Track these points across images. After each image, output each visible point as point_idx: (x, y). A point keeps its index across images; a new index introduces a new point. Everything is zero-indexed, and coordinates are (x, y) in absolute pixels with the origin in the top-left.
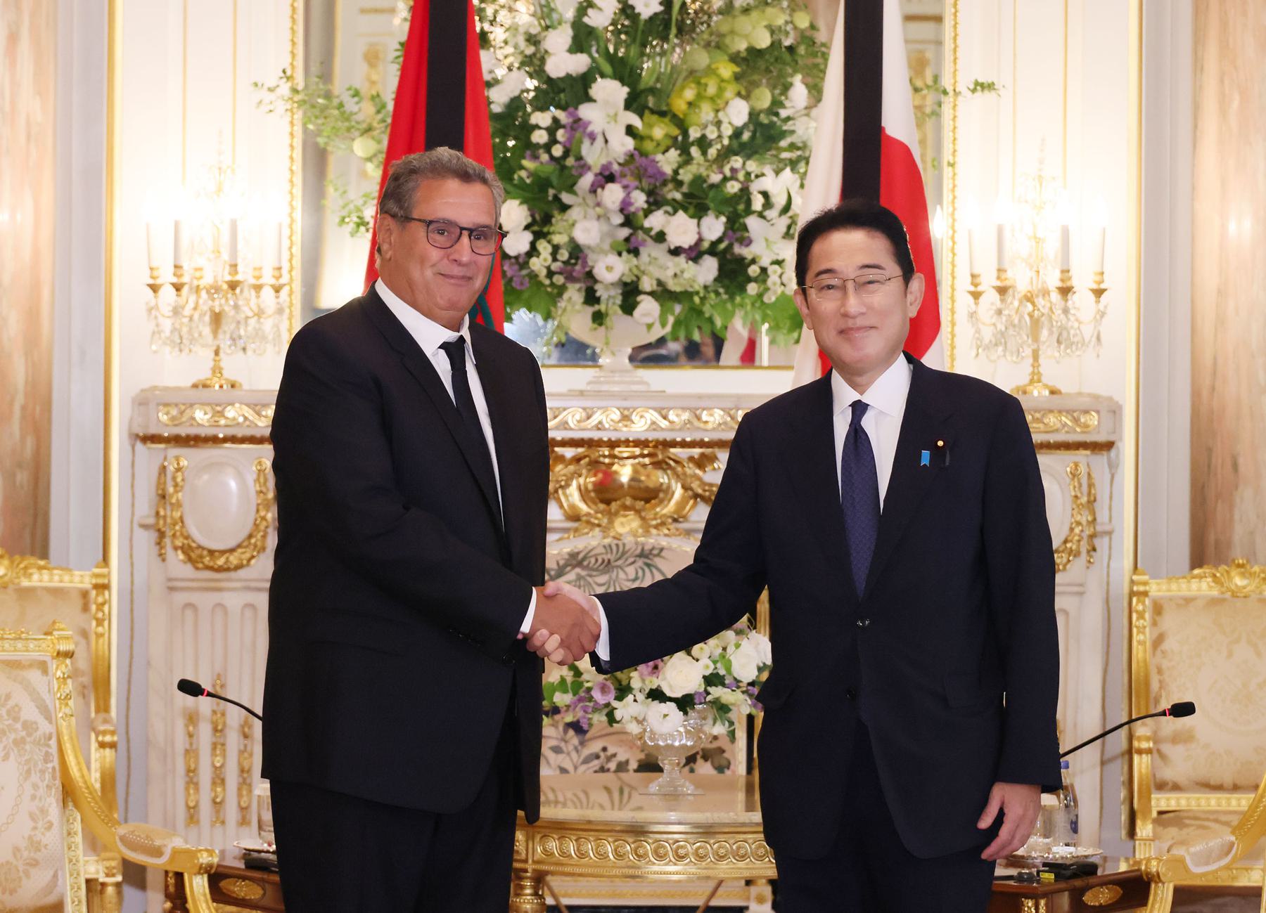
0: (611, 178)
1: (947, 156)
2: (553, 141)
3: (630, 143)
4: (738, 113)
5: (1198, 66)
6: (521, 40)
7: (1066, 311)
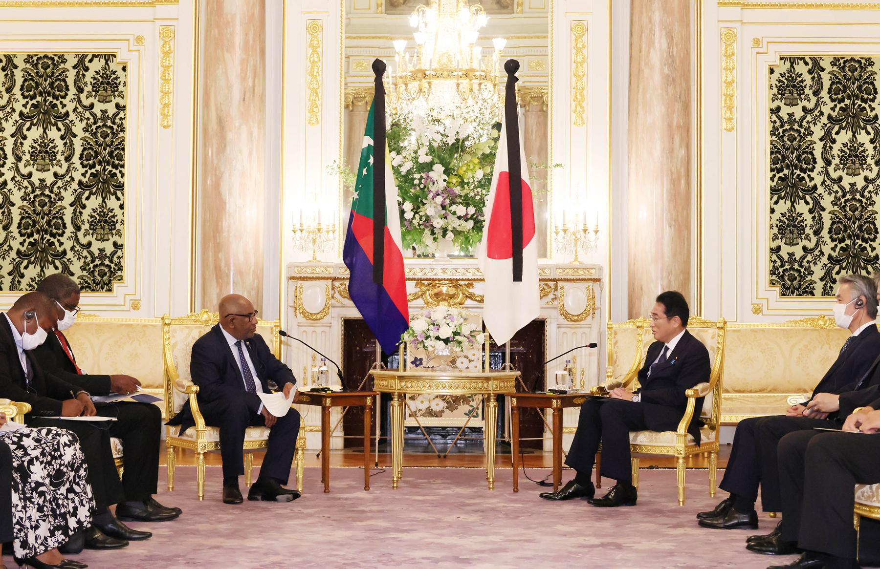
0: (439, 195)
1: (549, 189)
2: (421, 183)
3: (445, 184)
4: (479, 174)
5: (629, 162)
6: (412, 153)
7: (585, 237)
